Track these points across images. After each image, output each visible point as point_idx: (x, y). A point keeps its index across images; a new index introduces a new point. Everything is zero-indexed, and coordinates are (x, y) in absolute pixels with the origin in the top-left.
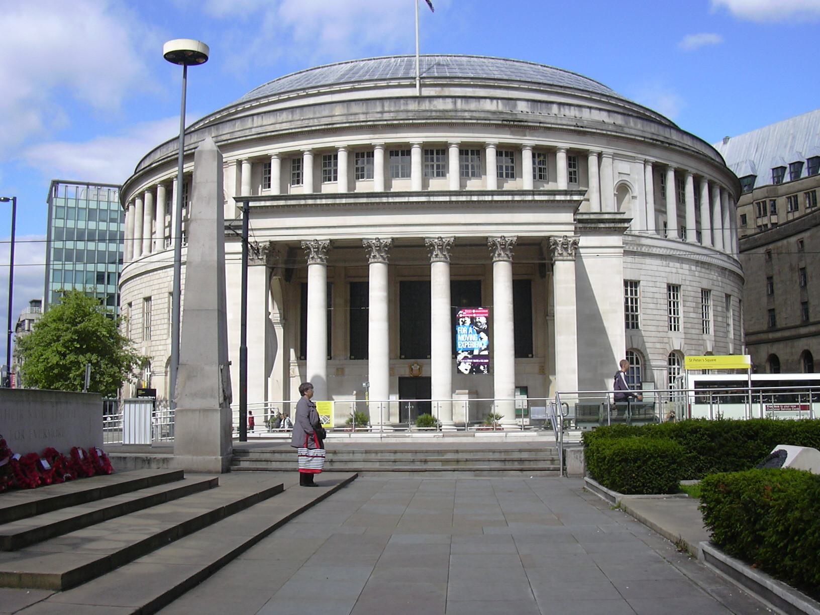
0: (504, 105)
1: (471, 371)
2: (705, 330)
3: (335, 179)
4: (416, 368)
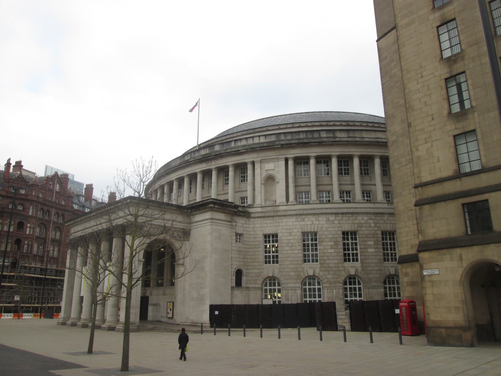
0: (209, 150)
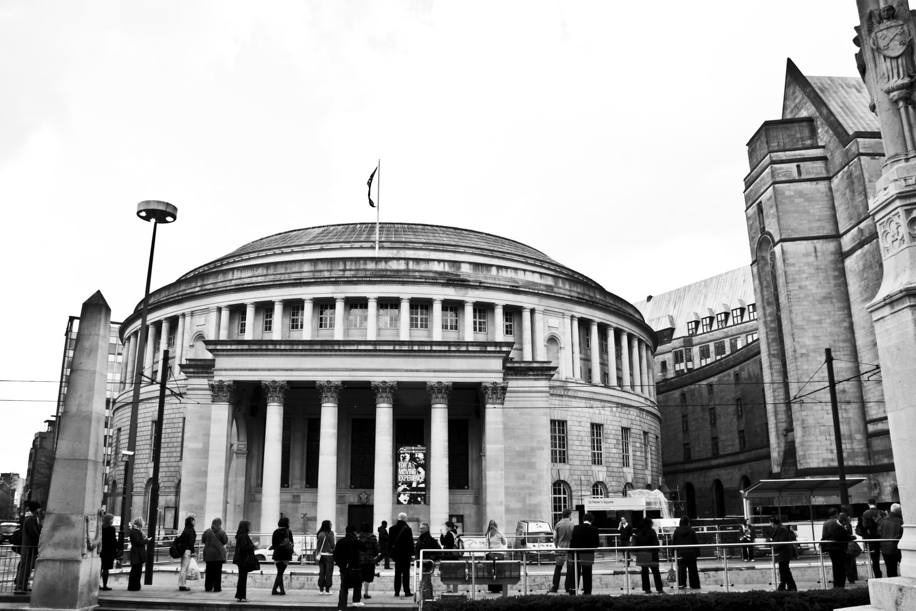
1: (409, 502)
2: (626, 464)
3: (302, 327)
4: (364, 496)
